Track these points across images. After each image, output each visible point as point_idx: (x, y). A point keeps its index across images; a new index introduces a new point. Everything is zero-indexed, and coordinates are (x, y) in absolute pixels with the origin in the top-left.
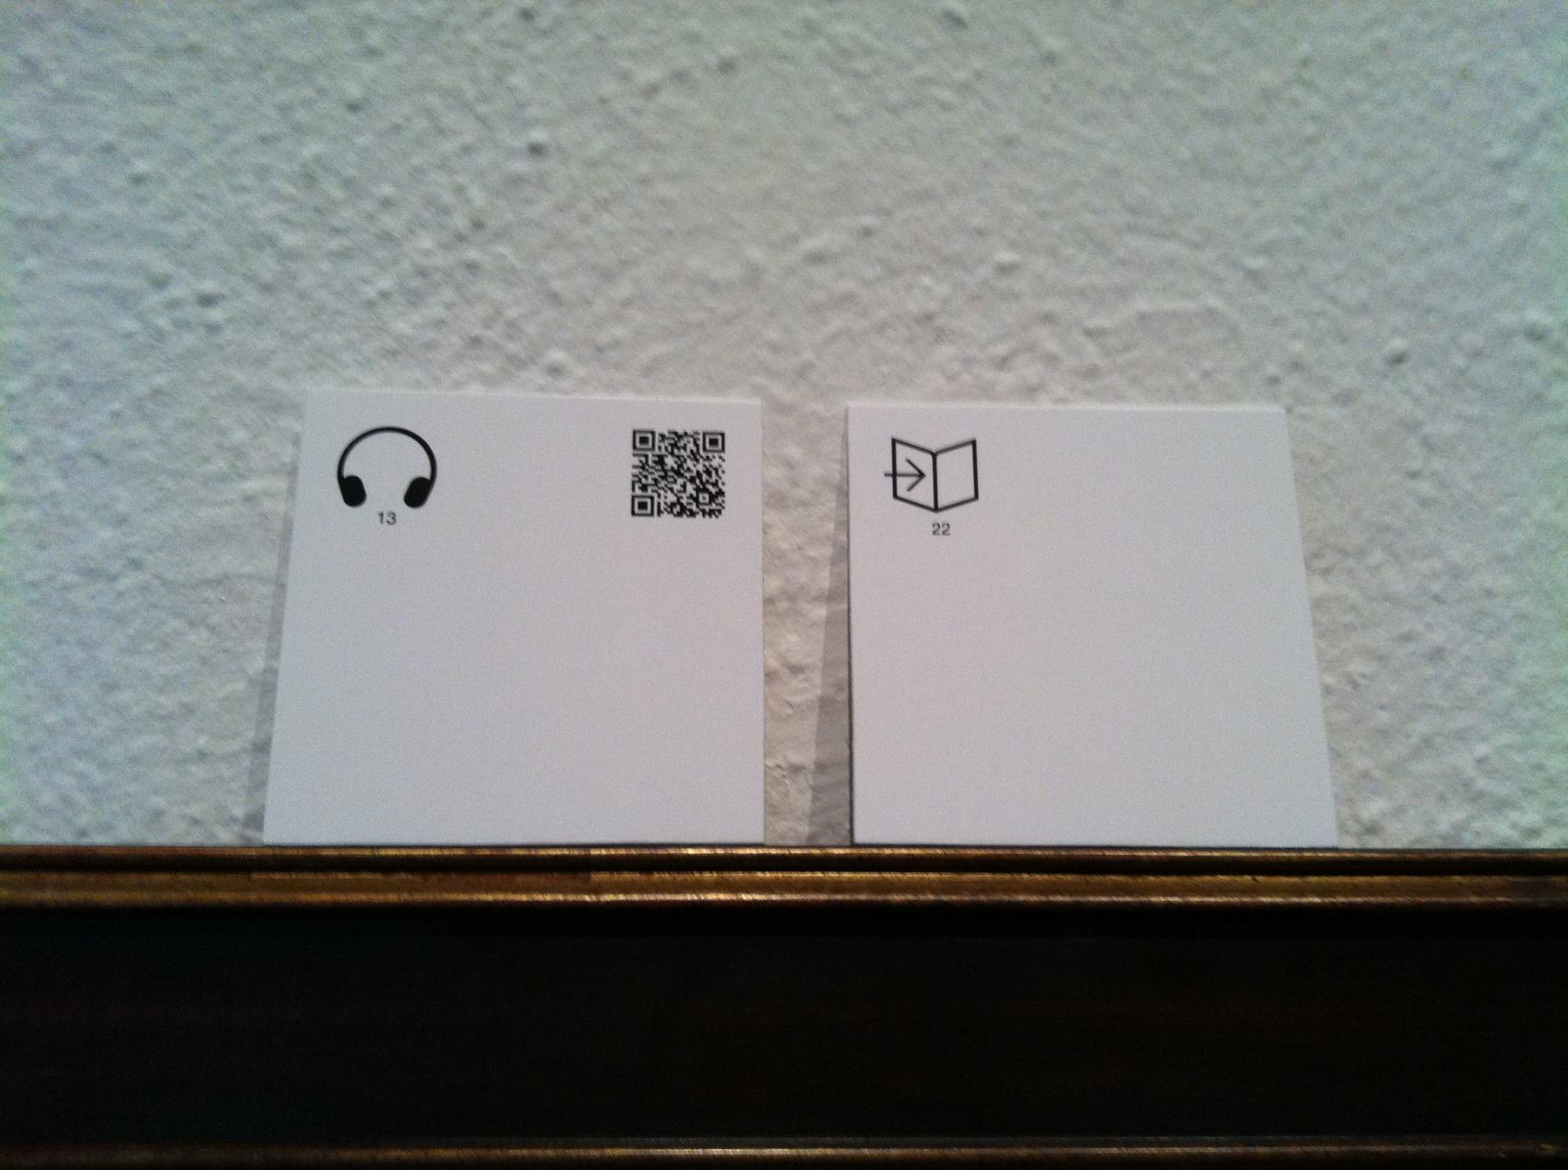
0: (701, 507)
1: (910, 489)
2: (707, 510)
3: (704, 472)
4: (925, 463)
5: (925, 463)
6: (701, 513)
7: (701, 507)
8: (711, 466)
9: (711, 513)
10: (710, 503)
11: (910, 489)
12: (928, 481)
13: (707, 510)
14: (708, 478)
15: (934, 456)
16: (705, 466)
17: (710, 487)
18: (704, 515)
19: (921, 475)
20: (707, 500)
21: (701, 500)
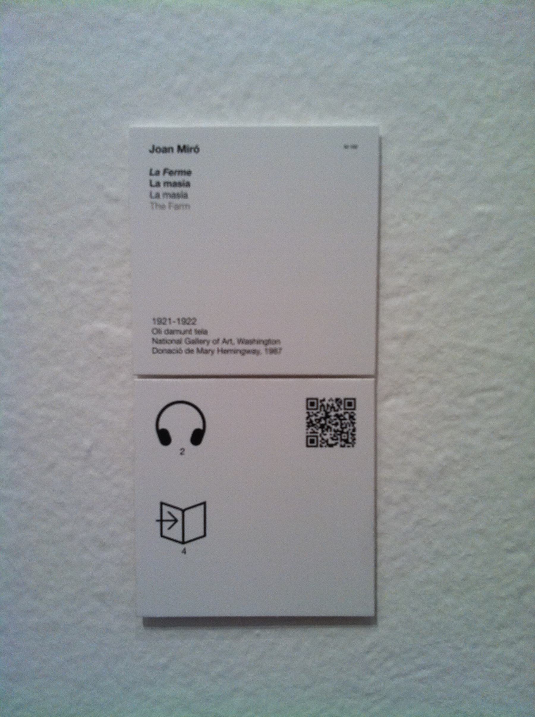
1: (170, 528)
4: (178, 514)
5: (178, 514)
11: (170, 528)
19: (176, 521)
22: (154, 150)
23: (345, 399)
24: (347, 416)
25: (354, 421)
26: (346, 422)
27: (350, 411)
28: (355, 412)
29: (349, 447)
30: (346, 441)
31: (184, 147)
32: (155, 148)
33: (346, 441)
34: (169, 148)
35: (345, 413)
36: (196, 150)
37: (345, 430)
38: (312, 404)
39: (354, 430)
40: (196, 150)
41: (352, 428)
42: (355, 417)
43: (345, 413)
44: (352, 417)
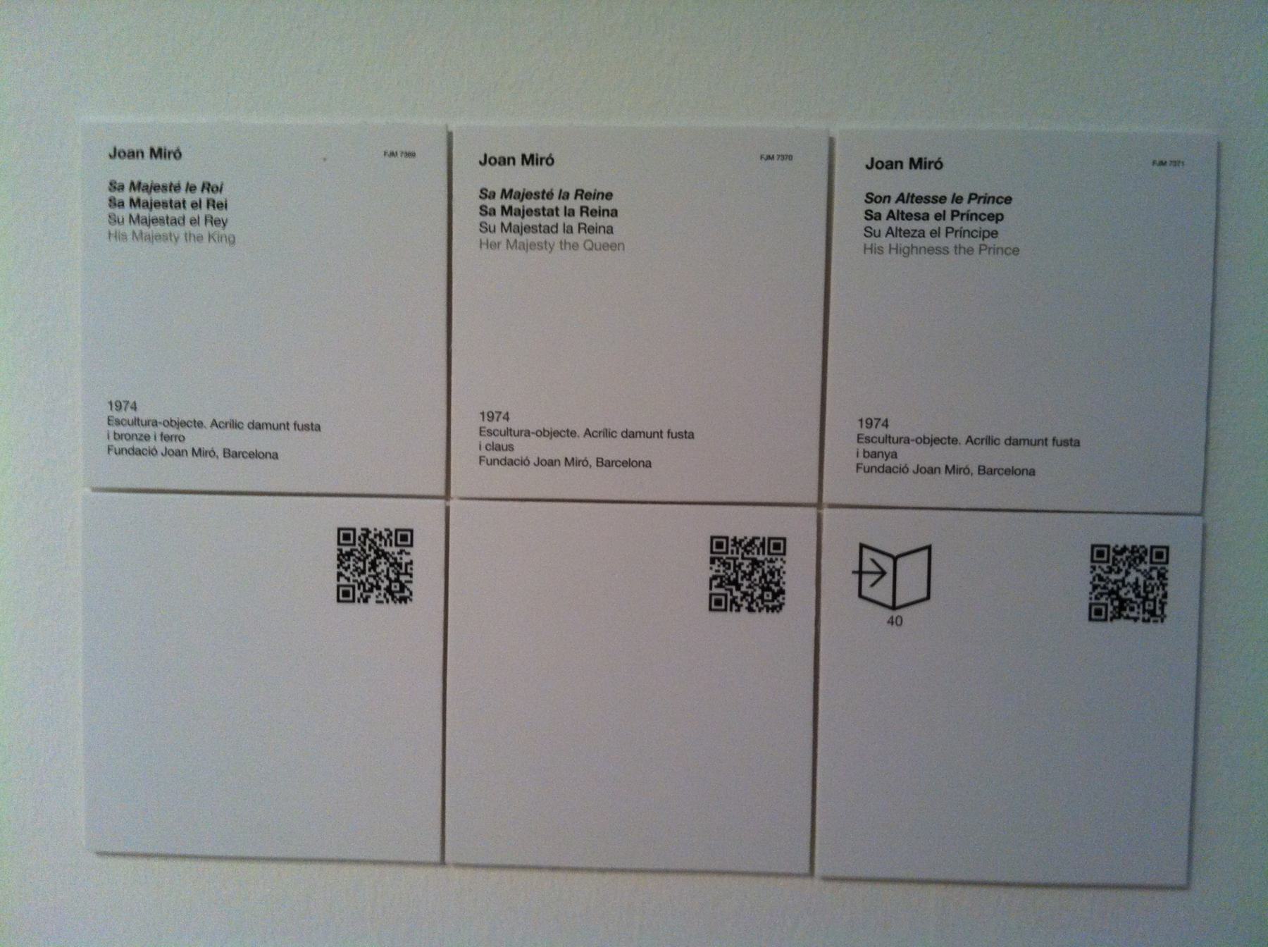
0: (765, 603)
2: (770, 606)
3: (768, 572)
6: (765, 609)
7: (765, 603)
8: (774, 567)
9: (773, 609)
10: (773, 601)
12: (888, 578)
13: (770, 606)
14: (771, 577)
15: (895, 559)
16: (768, 567)
17: (773, 586)
18: (767, 611)
20: (770, 598)
21: (765, 598)
22: (873, 164)
23: (1152, 547)
24: (1154, 574)
25: (1164, 582)
26: (1153, 582)
27: (1159, 566)
28: (1167, 567)
29: (1156, 621)
30: (1153, 613)
31: (920, 160)
32: (875, 161)
33: (1153, 613)
34: (896, 162)
35: (1151, 569)
36: (938, 165)
37: (1151, 596)
38: (1100, 554)
39: (1165, 596)
40: (938, 165)
41: (1161, 592)
42: (1167, 575)
43: (1151, 569)
44: (1162, 576)
